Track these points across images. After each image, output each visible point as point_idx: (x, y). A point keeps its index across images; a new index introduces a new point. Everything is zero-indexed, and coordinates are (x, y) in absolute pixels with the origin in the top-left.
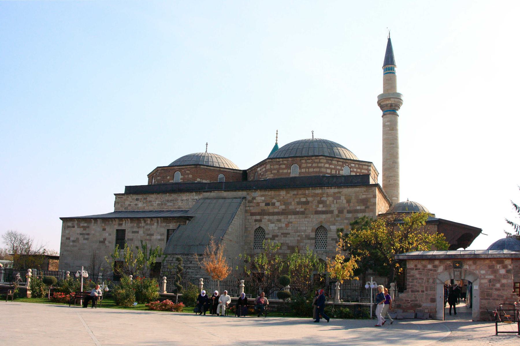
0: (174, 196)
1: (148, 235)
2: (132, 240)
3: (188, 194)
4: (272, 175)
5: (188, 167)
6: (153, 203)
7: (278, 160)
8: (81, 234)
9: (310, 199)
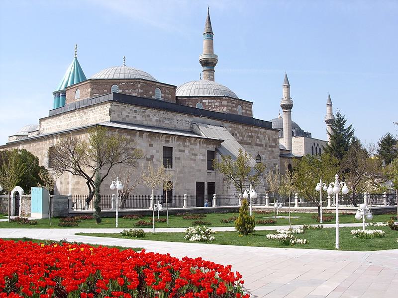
0: (170, 115)
1: (193, 154)
2: (179, 159)
3: (182, 115)
4: (228, 111)
7: (231, 99)
9: (253, 134)
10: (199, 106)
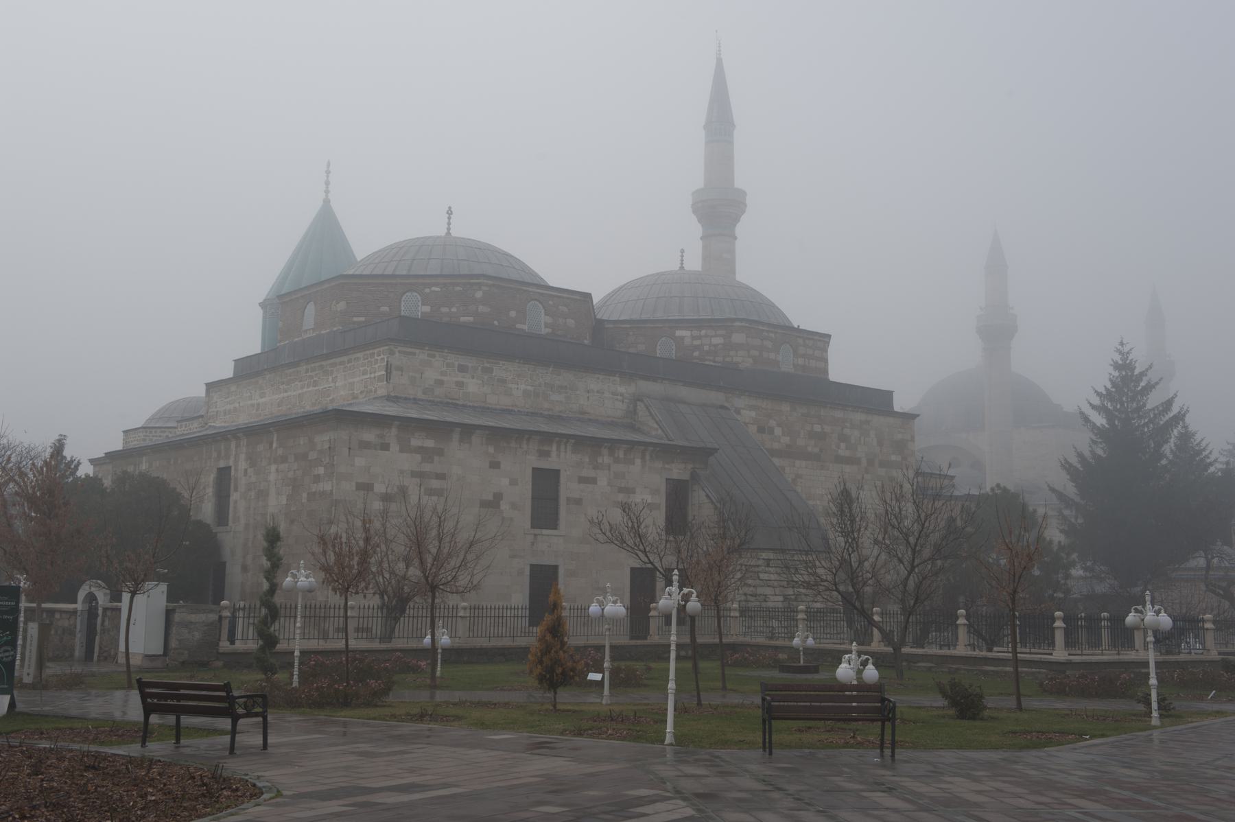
1: (621, 490)
2: (578, 502)
5: (565, 295)
6: (511, 388)
8: (414, 474)
9: (827, 429)
10: (665, 349)
